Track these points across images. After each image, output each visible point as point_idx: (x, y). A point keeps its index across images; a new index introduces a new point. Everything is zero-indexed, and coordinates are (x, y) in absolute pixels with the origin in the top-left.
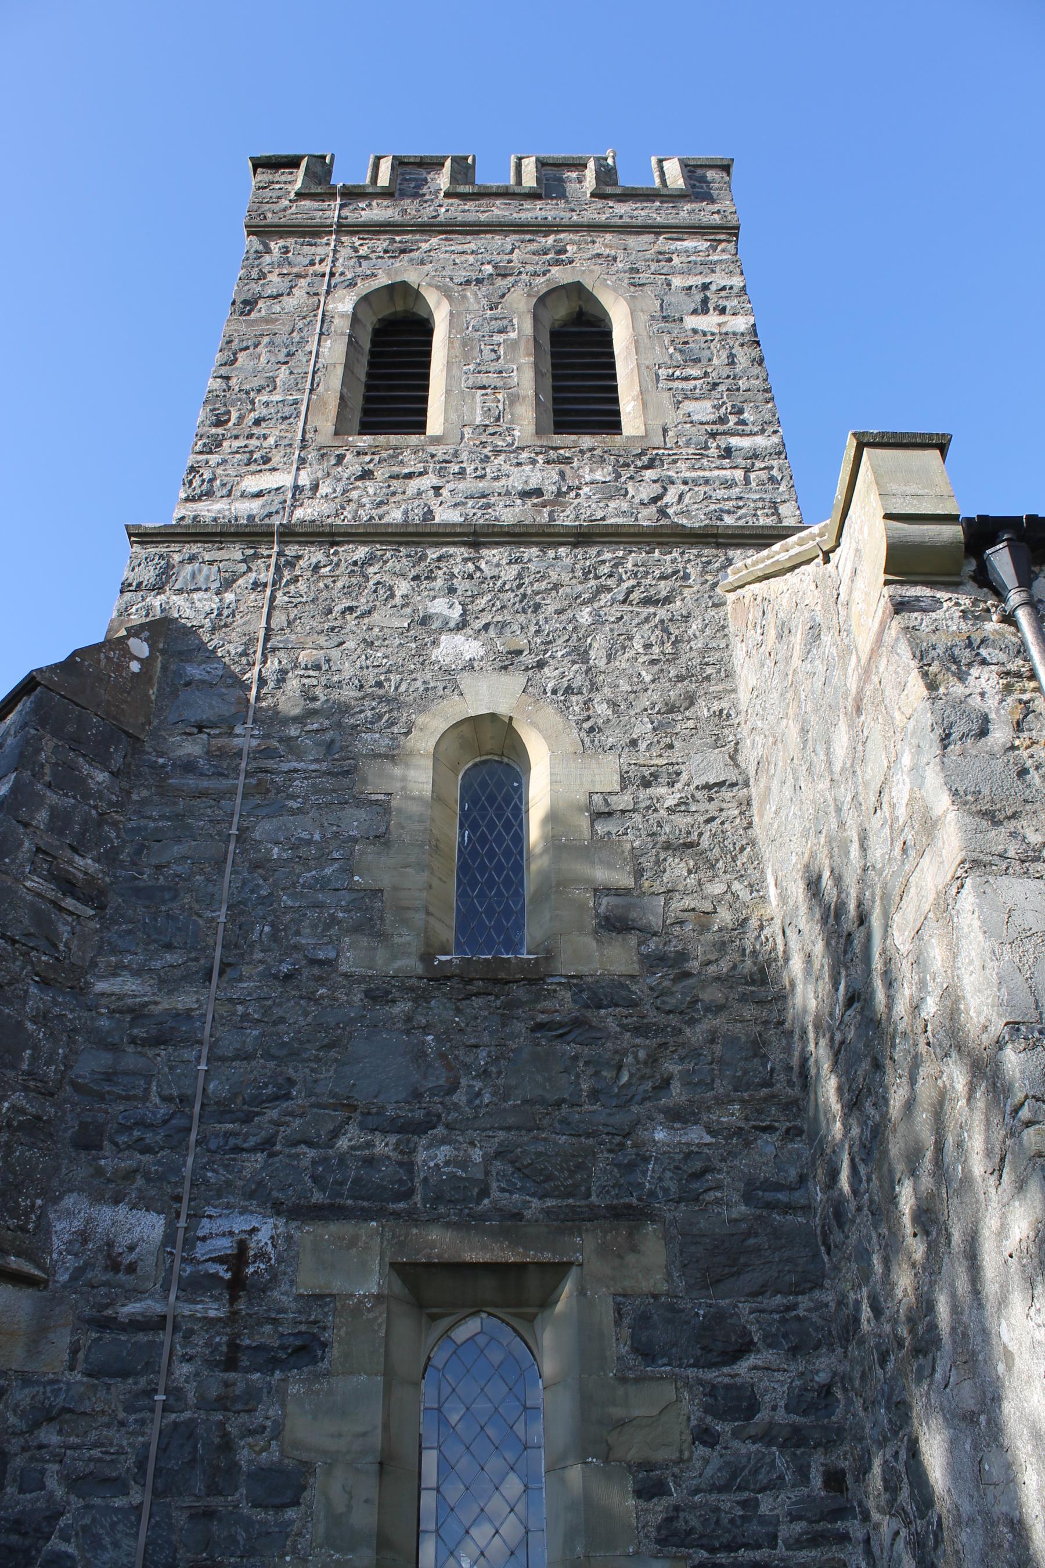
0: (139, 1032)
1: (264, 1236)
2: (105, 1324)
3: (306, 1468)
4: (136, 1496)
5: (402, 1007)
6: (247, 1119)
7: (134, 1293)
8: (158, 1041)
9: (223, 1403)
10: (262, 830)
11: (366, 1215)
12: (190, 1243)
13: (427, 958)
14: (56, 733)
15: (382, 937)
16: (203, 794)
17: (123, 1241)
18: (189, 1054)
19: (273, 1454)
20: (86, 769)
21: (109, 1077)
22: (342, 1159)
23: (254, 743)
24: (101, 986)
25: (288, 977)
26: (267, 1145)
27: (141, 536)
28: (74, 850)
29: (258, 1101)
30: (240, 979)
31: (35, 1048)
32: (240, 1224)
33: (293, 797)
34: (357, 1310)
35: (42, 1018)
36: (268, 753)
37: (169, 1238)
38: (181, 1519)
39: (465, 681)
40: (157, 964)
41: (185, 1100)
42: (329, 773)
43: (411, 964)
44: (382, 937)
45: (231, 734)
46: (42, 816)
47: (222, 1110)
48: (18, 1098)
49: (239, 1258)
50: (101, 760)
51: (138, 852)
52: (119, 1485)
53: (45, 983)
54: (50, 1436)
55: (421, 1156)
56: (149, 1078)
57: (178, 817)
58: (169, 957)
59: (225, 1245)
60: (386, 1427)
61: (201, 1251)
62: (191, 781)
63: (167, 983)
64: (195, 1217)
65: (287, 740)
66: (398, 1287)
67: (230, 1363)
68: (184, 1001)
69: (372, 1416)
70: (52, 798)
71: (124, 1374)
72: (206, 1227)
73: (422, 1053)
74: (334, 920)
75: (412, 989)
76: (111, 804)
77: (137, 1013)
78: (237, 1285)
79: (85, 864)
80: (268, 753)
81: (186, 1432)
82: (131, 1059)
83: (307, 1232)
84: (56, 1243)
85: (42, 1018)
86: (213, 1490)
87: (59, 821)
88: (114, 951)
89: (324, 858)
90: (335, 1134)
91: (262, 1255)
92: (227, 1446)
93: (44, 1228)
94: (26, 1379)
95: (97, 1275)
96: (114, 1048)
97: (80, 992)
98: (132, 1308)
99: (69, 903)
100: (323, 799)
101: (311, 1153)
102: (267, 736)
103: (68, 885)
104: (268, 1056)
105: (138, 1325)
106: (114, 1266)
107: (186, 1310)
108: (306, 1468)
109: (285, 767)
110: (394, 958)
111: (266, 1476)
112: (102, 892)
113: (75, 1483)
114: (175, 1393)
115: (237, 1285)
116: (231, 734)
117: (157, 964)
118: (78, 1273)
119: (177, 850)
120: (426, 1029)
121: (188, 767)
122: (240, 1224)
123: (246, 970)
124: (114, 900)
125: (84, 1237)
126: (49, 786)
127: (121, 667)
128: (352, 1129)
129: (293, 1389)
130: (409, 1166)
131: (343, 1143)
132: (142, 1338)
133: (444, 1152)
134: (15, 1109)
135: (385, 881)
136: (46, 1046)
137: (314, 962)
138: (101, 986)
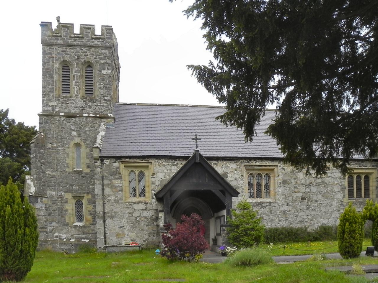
1: (62, 194)
2: (53, 200)
5: (71, 175)
7: (54, 198)
9: (61, 206)
10: (58, 156)
11: (69, 192)
12: (57, 194)
15: (69, 168)
16: (52, 152)
18: (55, 179)
19: (65, 209)
24: (47, 172)
26: (62, 187)
35: (43, 176)
37: (56, 194)
39: (75, 138)
42: (63, 150)
43: (71, 170)
44: (69, 168)
47: (58, 184)
49: (61, 195)
50: (42, 149)
53: (42, 173)
56: (52, 181)
58: (52, 170)
59: (60, 195)
61: (58, 195)
62: (50, 150)
63: (52, 172)
64: (57, 192)
66: (72, 198)
67: (61, 203)
68: (54, 174)
72: (58, 193)
73: (73, 179)
77: (50, 175)
83: (66, 194)
85: (43, 176)
88: (47, 169)
89: (63, 159)
92: (62, 208)
93: (47, 193)
94: (48, 204)
97: (45, 173)
99: (42, 165)
100: (63, 153)
102: (57, 145)
103: (42, 163)
111: (65, 210)
113: (52, 210)
115: (61, 197)
119: (51, 158)
120: (73, 177)
124: (46, 164)
125: (50, 194)
131: (67, 186)
133: (75, 187)
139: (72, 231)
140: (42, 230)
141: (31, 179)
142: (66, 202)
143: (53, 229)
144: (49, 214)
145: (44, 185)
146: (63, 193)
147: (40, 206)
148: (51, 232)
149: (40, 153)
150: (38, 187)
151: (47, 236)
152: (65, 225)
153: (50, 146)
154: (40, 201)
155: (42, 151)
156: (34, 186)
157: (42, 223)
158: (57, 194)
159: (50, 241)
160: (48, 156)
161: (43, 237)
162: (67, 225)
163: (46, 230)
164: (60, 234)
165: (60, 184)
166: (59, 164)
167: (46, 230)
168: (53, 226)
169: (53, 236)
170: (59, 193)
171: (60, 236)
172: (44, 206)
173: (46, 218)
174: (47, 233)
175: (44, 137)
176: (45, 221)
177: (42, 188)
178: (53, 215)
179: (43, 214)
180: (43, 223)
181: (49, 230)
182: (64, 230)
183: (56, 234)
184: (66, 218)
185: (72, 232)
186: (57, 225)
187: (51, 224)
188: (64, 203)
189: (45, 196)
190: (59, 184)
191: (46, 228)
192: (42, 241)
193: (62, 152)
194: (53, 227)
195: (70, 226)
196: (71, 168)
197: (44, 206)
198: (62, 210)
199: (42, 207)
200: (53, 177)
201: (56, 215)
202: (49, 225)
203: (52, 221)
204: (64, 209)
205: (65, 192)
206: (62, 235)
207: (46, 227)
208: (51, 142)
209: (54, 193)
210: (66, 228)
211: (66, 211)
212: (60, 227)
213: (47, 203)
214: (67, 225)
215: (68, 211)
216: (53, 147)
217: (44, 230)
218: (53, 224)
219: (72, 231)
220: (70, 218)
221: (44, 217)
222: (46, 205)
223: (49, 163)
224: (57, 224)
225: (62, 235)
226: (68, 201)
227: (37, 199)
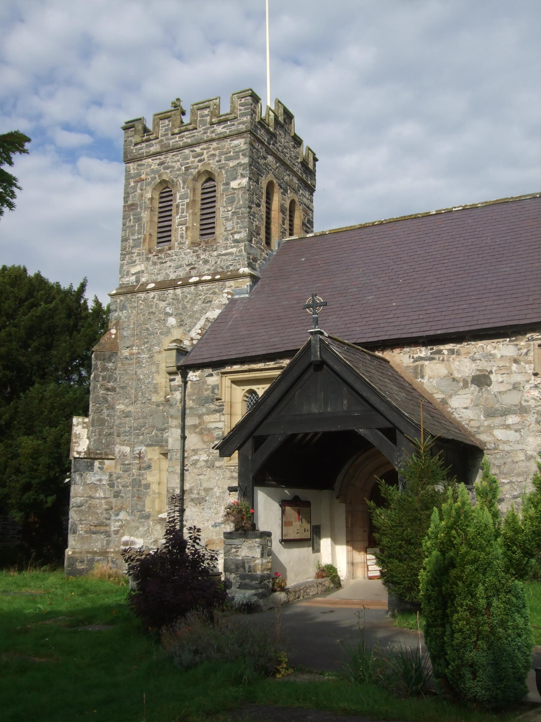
0: (124, 415)
1: (143, 450)
2: (124, 464)
3: (150, 484)
4: (130, 488)
5: (161, 408)
6: (140, 430)
7: (127, 460)
8: (126, 417)
9: (139, 475)
10: (139, 372)
11: (156, 446)
12: (133, 451)
13: (165, 397)
14: (100, 360)
15: (158, 393)
16: (129, 364)
17: (125, 452)
18: (131, 419)
20: (107, 364)
21: (120, 424)
22: (153, 436)
23: (136, 351)
24: (117, 407)
25: (144, 403)
26: (143, 434)
27: (111, 296)
28: (108, 382)
29: (141, 427)
30: (137, 404)
31: (108, 422)
32: (140, 448)
33: (143, 364)
34: (155, 461)
35: (108, 416)
36: (139, 353)
37: (131, 451)
38: (135, 491)
39: (172, 330)
40: (125, 402)
41: (131, 427)
43: (163, 399)
44: (158, 393)
45: (132, 349)
46: (101, 378)
48: (106, 430)
49: (140, 454)
50: (110, 360)
51: (120, 379)
52: (127, 487)
54: (119, 480)
55: (164, 435)
56: (126, 423)
57: (126, 370)
58: (127, 401)
59: (138, 452)
60: (160, 478)
61: (135, 453)
62: (127, 362)
65: (142, 349)
67: (140, 469)
69: (158, 476)
70: (102, 374)
71: (127, 471)
72: (135, 449)
73: (164, 416)
74: (151, 391)
75: (163, 404)
76: (114, 370)
78: (140, 458)
79: (110, 385)
80: (139, 353)
81: (135, 479)
82: (123, 421)
83: (149, 449)
84: (116, 453)
85: (108, 416)
86: (139, 487)
87: (104, 378)
90: (152, 432)
91: (143, 453)
92: (140, 481)
95: (122, 457)
96: (121, 418)
98: (127, 462)
99: (109, 393)
100: (148, 364)
101: (149, 435)
102: (138, 349)
103: (108, 389)
104: (142, 418)
105: (128, 464)
106: (124, 456)
107: (134, 462)
108: (150, 484)
109: (142, 356)
110: (160, 398)
111: (145, 485)
112: (115, 388)
113: (123, 486)
114: (133, 474)
115: (140, 458)
116: (132, 349)
117: (125, 402)
118: (120, 456)
121: (126, 358)
122: (140, 448)
123: (138, 402)
124: (118, 389)
125: (120, 451)
126: (101, 372)
127: (110, 338)
128: (155, 430)
129: (148, 473)
130: (162, 437)
131: (153, 433)
132: (129, 466)
134: (106, 433)
135: (159, 381)
136: (110, 420)
137: (148, 400)
138: (117, 407)
139: (157, 530)
140: (98, 528)
141: (85, 423)
142: (149, 467)
143: (121, 526)
144: (117, 495)
145: (110, 434)
146: (143, 449)
147: (98, 478)
148: (116, 532)
149: (105, 369)
150: (95, 440)
151: (108, 542)
152: (142, 517)
153: (126, 353)
154: (99, 468)
155: (111, 365)
156: (88, 438)
157: (98, 514)
158: (132, 451)
159: (112, 552)
160: (122, 374)
161: (99, 544)
162: (147, 517)
163: (107, 528)
164: (132, 538)
165: (140, 430)
166: (141, 387)
167: (107, 528)
168: (121, 520)
169: (119, 541)
170: (137, 449)
171: (133, 543)
172: (105, 478)
173: (108, 503)
174: (109, 536)
175: (116, 338)
176: (107, 510)
177: (106, 439)
178: (122, 497)
179: (102, 495)
180: (102, 513)
181: (113, 529)
182: (141, 529)
183: (125, 538)
184: (146, 501)
185: (155, 533)
186: (128, 518)
187: (117, 515)
188: (145, 469)
189: (110, 457)
190: (137, 429)
191: (106, 526)
192: (95, 553)
193: (147, 362)
194: (120, 523)
195: (153, 521)
196: (162, 394)
197: (107, 478)
198: (140, 485)
199: (100, 480)
200: (127, 415)
201: (127, 496)
202: (113, 518)
203: (121, 509)
204: (143, 482)
205: (148, 446)
206: (136, 540)
207: (108, 522)
208: (128, 345)
209: (127, 449)
210: (144, 525)
211: (147, 486)
212: (133, 521)
213: (113, 470)
214: (147, 517)
215: (151, 486)
216: (131, 354)
217: (103, 529)
218: (123, 515)
219: (157, 530)
220: (153, 502)
221: (103, 501)
222: (111, 475)
223: (123, 388)
224: (129, 515)
225: (136, 540)
226: (153, 465)
227: (92, 465)
